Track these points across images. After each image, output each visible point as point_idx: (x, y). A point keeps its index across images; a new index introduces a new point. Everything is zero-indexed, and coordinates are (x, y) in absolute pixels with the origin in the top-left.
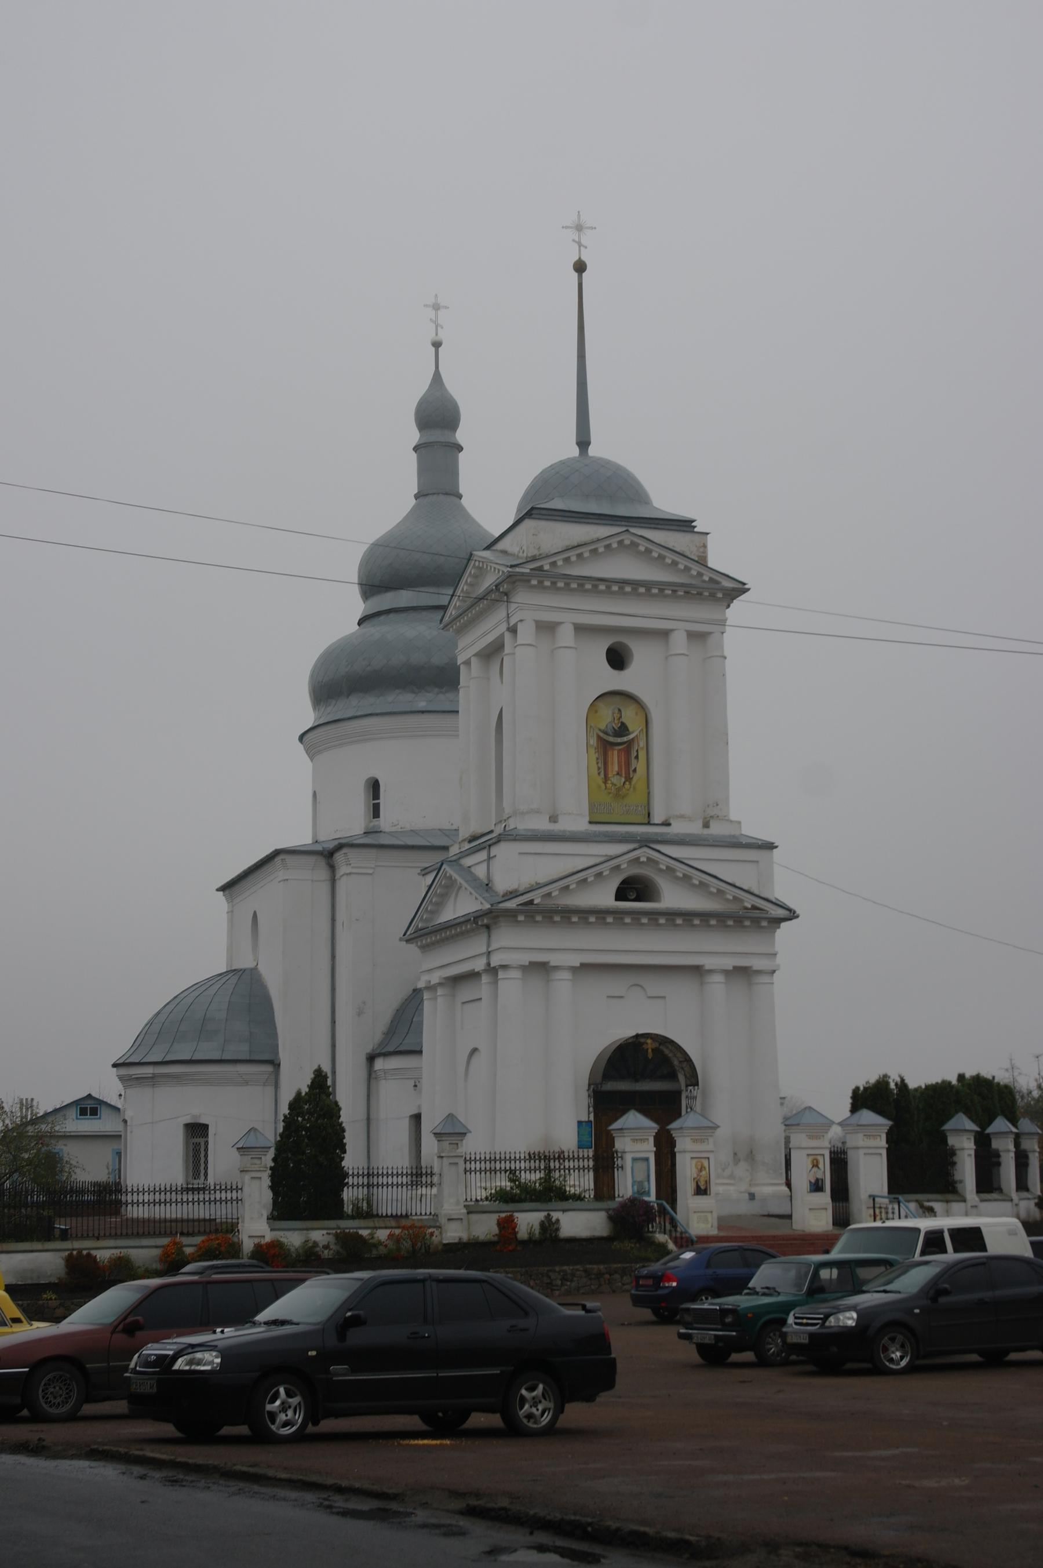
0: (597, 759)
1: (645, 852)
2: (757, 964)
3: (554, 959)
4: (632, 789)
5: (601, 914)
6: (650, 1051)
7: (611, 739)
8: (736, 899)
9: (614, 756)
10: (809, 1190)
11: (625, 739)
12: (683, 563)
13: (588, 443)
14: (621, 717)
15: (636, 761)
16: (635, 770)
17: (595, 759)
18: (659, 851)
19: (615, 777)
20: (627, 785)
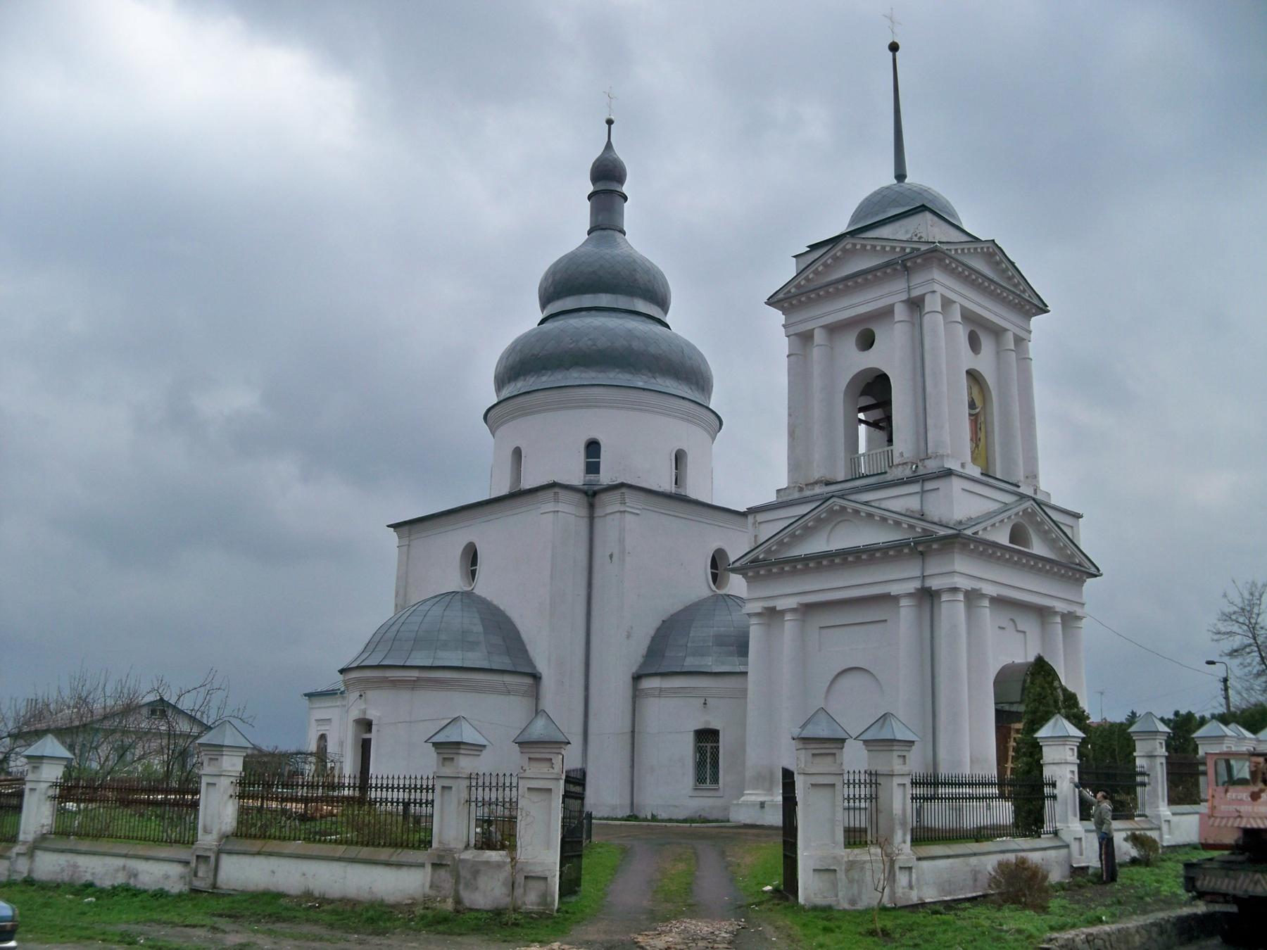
1: (834, 502)
2: (935, 584)
3: (781, 604)
8: (911, 527)
13: (905, 177)
18: (844, 499)
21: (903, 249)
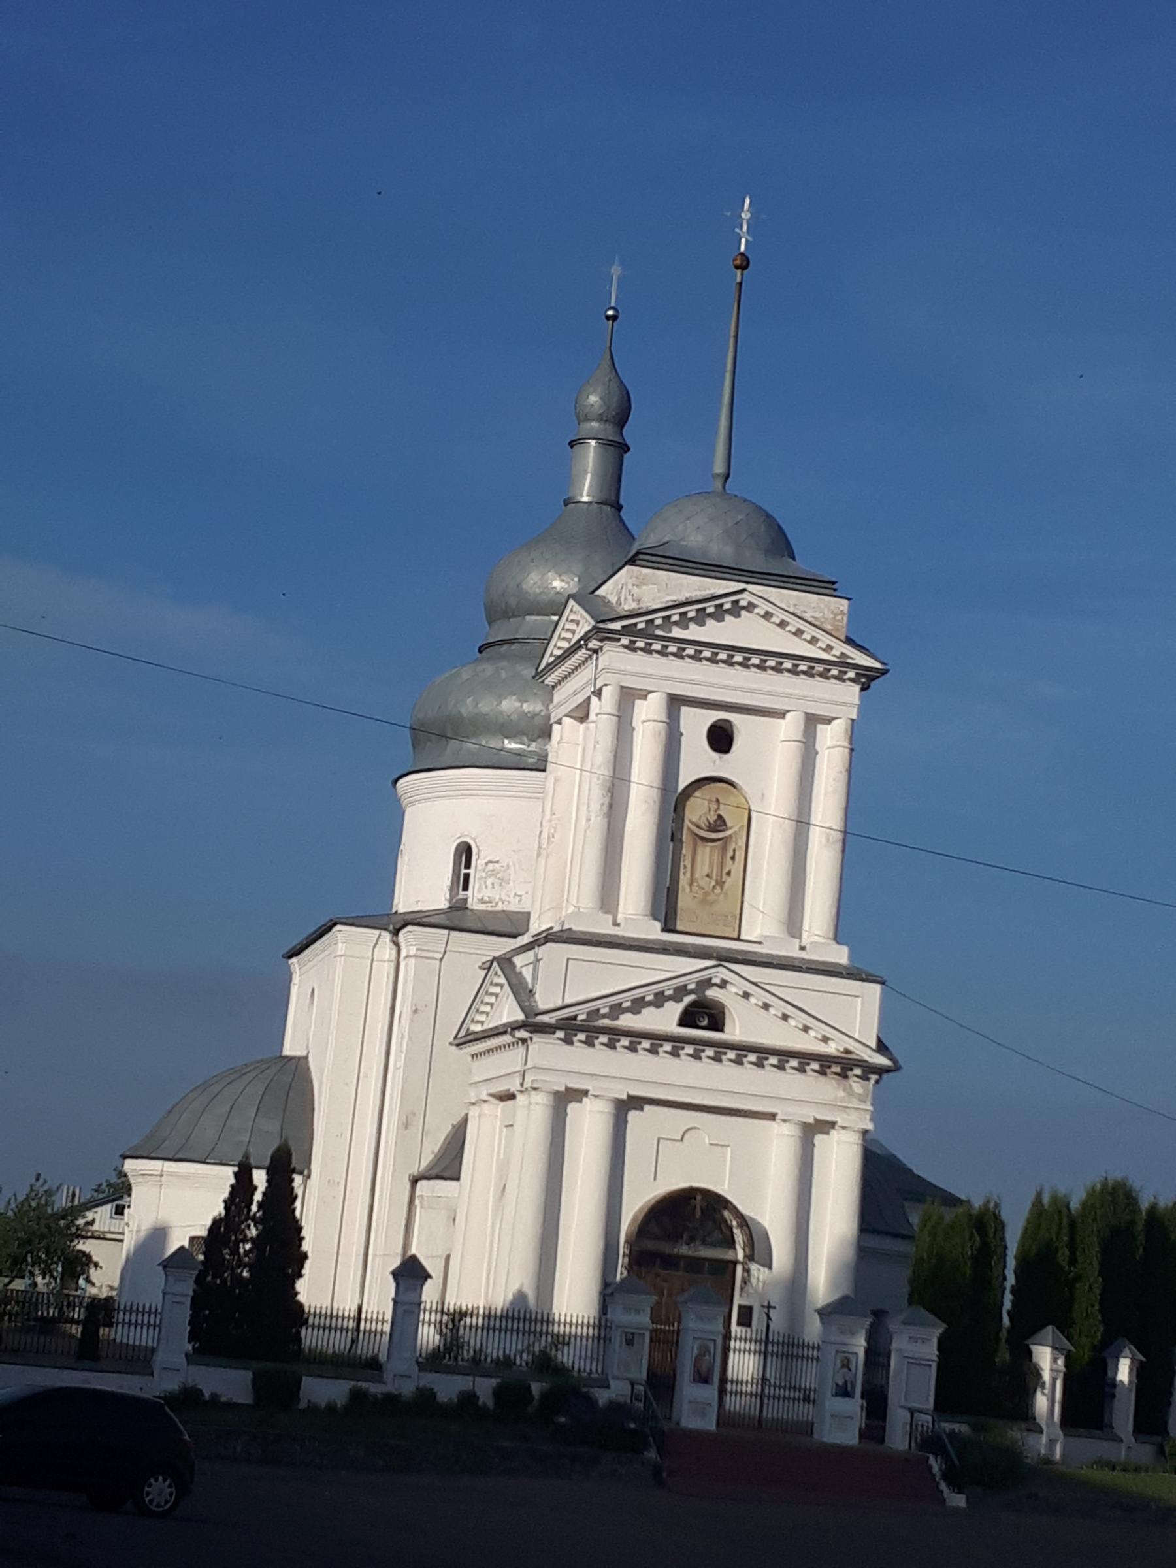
4: (722, 896)
5: (657, 1039)
6: (698, 1208)
10: (834, 1393)
11: (721, 835)
12: (809, 632)
14: (718, 808)
15: (731, 862)
16: (729, 873)
20: (718, 891)
21: (829, 648)
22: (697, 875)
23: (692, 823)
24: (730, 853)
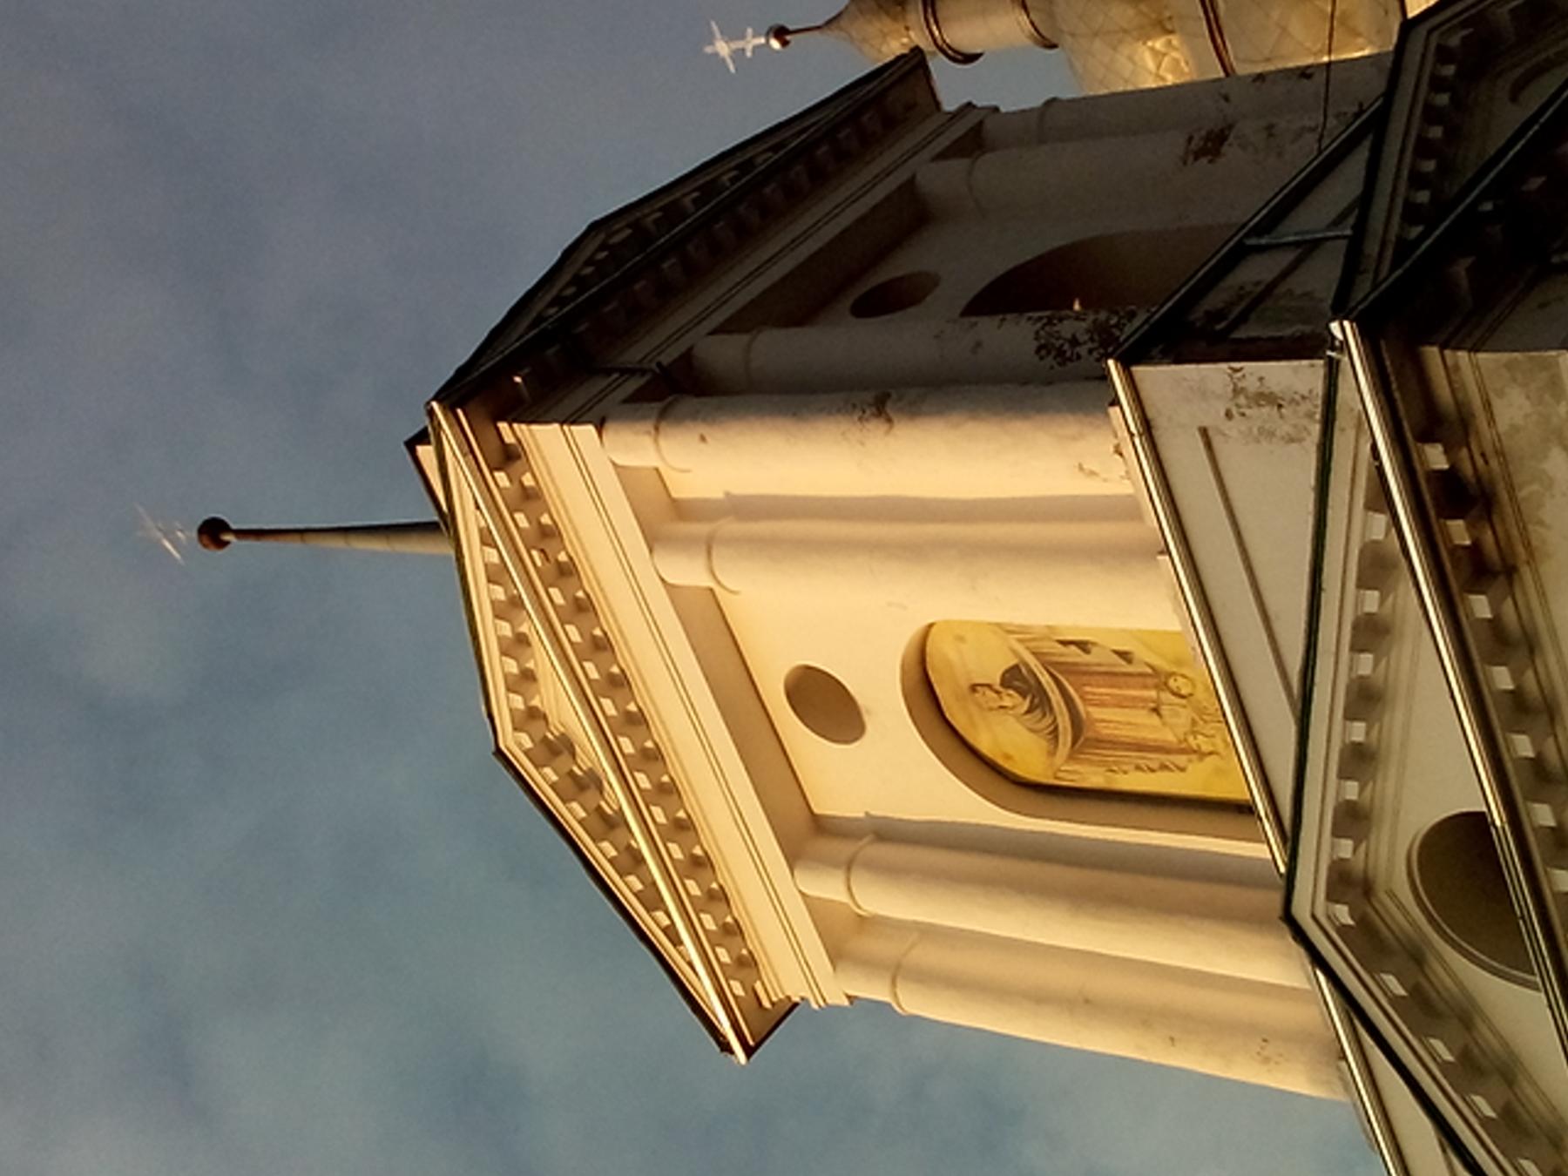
0: (1138, 768)
7: (1064, 721)
9: (1108, 718)
14: (989, 686)
15: (1094, 650)
16: (1124, 655)
17: (1140, 774)
19: (1167, 719)
22: (1169, 737)
23: (1052, 753)
24: (1074, 655)
